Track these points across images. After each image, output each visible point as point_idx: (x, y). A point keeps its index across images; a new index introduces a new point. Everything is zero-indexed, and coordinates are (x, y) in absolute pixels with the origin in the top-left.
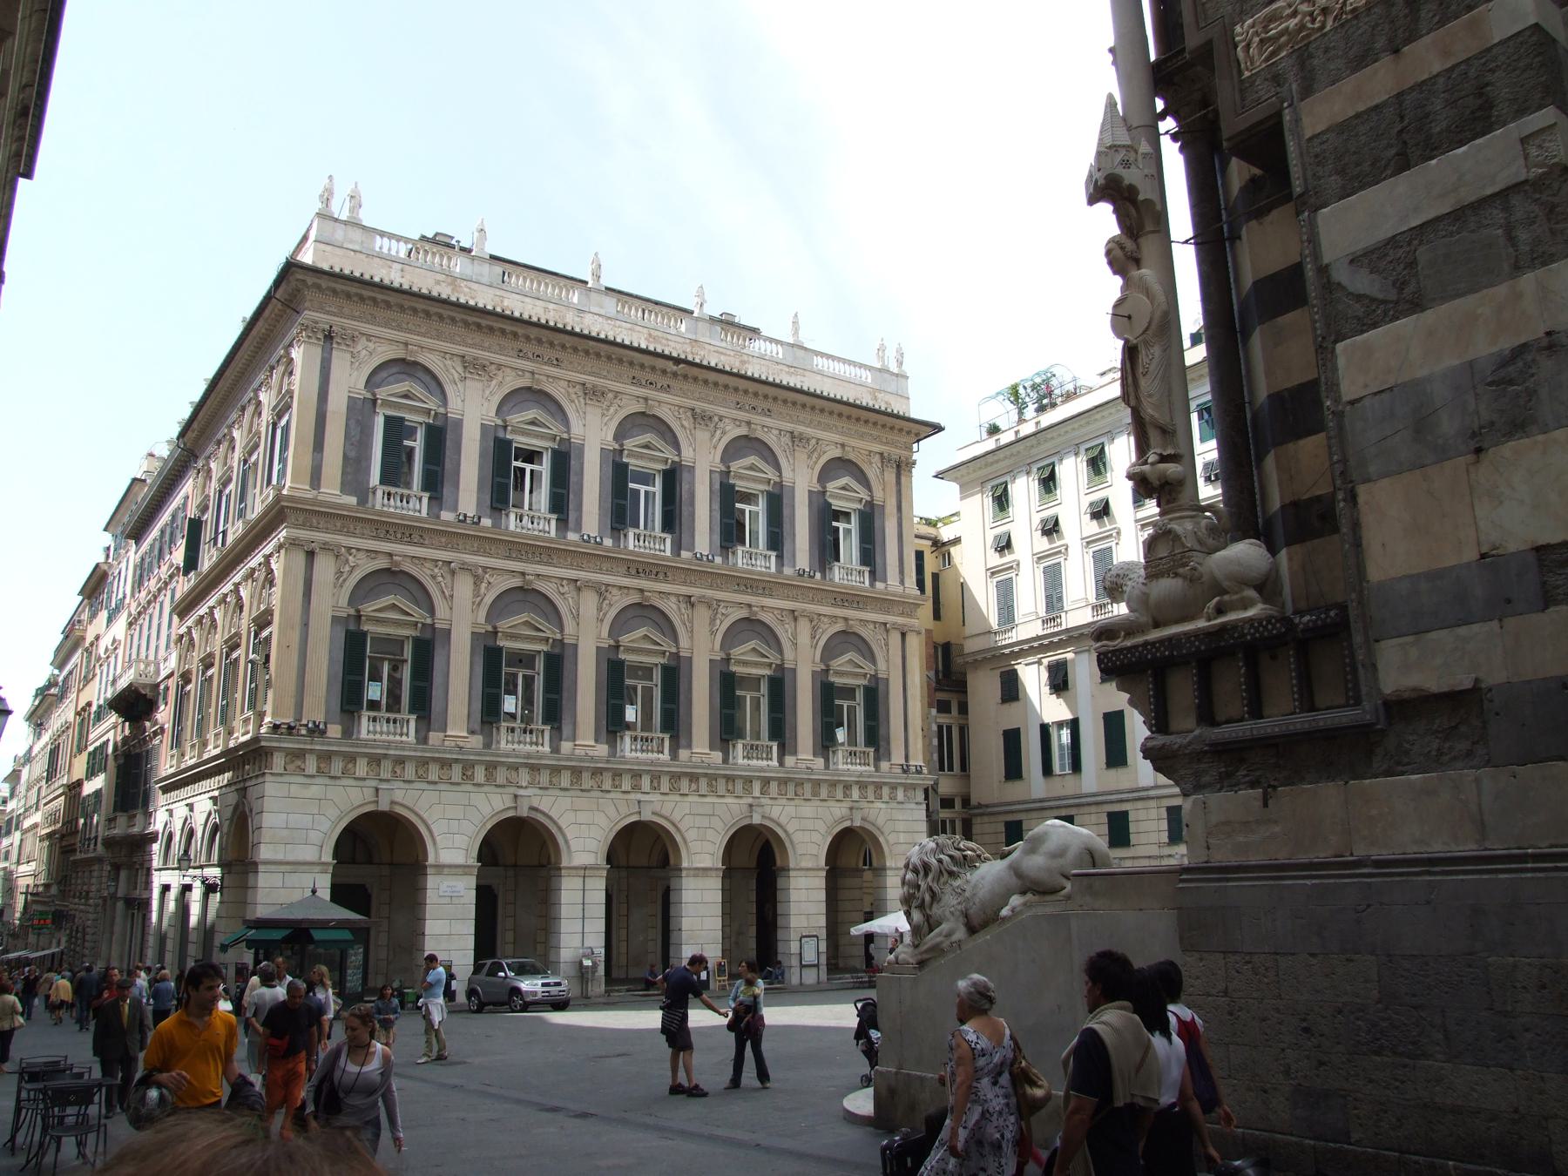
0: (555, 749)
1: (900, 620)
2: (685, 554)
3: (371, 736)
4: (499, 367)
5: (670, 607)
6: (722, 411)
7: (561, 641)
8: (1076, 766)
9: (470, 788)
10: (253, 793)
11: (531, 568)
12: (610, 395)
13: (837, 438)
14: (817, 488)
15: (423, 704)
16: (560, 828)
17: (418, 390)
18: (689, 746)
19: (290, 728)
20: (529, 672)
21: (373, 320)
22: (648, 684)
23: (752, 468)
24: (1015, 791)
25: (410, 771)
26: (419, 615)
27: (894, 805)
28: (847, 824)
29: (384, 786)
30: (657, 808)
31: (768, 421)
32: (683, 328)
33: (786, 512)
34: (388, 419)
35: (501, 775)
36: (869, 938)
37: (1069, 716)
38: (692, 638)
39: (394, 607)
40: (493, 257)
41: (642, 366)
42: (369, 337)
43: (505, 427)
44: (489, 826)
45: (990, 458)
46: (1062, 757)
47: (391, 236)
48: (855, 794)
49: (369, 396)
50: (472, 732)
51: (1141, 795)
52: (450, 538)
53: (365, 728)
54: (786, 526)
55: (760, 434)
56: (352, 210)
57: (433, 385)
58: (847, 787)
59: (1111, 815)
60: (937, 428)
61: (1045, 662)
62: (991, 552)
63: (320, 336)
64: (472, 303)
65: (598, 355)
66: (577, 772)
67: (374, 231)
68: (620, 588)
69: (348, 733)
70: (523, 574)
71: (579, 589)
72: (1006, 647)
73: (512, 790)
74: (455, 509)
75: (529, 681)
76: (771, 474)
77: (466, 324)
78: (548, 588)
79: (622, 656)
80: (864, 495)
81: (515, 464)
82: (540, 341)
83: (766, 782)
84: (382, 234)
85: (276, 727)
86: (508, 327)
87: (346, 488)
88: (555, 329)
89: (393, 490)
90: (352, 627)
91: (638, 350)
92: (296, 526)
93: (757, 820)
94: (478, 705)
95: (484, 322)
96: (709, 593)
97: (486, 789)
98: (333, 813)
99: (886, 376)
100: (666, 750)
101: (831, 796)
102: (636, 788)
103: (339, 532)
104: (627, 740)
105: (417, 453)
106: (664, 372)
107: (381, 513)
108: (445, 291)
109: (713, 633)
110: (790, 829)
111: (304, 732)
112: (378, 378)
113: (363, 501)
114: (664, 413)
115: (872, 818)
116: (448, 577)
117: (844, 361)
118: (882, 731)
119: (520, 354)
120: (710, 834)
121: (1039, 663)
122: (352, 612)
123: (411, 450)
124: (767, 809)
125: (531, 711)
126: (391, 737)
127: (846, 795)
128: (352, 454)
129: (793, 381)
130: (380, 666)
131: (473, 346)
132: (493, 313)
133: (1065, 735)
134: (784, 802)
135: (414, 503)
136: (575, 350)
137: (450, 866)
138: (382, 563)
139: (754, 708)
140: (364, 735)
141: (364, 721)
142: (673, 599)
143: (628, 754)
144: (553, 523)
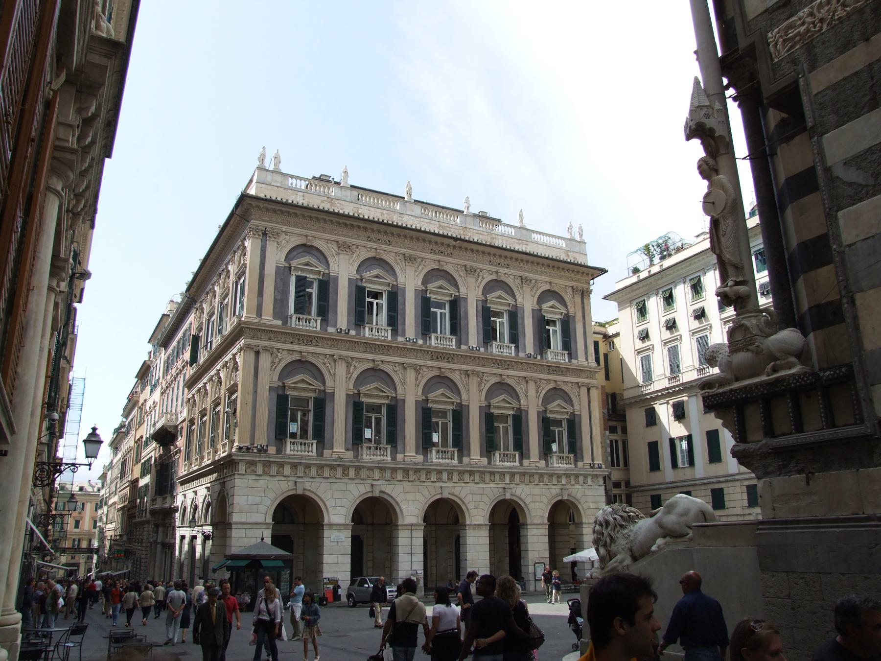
0: (394, 458)
1: (587, 381)
2: (463, 347)
3: (292, 453)
4: (358, 246)
5: (456, 377)
6: (481, 266)
7: (396, 397)
8: (691, 462)
9: (346, 481)
10: (228, 485)
11: (378, 357)
12: (419, 260)
13: (547, 279)
14: (536, 307)
15: (320, 434)
16: (397, 503)
17: (313, 261)
18: (469, 455)
19: (248, 449)
20: (378, 415)
21: (288, 224)
22: (444, 420)
23: (500, 297)
24: (656, 477)
25: (313, 472)
26: (317, 385)
27: (586, 487)
28: (559, 498)
29: (299, 480)
30: (451, 490)
31: (508, 271)
32: (458, 221)
33: (519, 321)
34: (297, 277)
35: (364, 473)
36: (574, 564)
37: (686, 433)
38: (468, 394)
39: (303, 381)
40: (352, 186)
41: (436, 243)
42: (286, 233)
43: (362, 280)
44: (358, 502)
45: (635, 287)
46: (683, 457)
47: (297, 178)
48: (564, 480)
49: (287, 265)
50: (347, 450)
51: (730, 479)
52: (333, 342)
53: (289, 448)
54: (520, 330)
55: (503, 278)
56: (275, 165)
57: (322, 257)
58: (559, 477)
59: (713, 491)
60: (604, 271)
61: (671, 402)
62: (637, 340)
63: (260, 233)
64: (341, 212)
65: (412, 238)
66: (406, 471)
67: (288, 175)
68: (428, 367)
69: (279, 451)
70: (374, 361)
71: (405, 368)
72: (648, 394)
73: (370, 482)
74: (335, 325)
75: (378, 421)
76: (510, 301)
77: (339, 224)
78: (387, 368)
79: (430, 405)
80: (563, 310)
81: (368, 300)
82: (379, 231)
83: (513, 475)
84: (292, 177)
85: (240, 448)
86: (362, 225)
87: (276, 316)
88: (387, 224)
89: (301, 316)
90: (280, 392)
91: (434, 234)
92: (250, 338)
93: (508, 496)
94: (350, 435)
95: (348, 222)
96: (478, 369)
97: (355, 481)
98: (272, 495)
99: (574, 243)
100: (456, 458)
101: (550, 482)
102: (439, 479)
103: (273, 340)
104: (434, 452)
105: (314, 296)
106: (449, 246)
107: (295, 329)
108: (327, 206)
109: (481, 391)
110: (527, 501)
111: (255, 451)
112: (291, 256)
113: (285, 323)
114: (450, 269)
115: (573, 494)
116: (333, 363)
117: (549, 235)
118: (578, 444)
119: (369, 239)
120: (482, 505)
121: (667, 403)
122: (280, 384)
123: (310, 294)
124: (514, 490)
125: (380, 437)
126: (303, 453)
127: (558, 482)
128: (279, 297)
129: (521, 248)
130: (296, 414)
131: (344, 235)
132: (353, 217)
133: (684, 444)
134: (524, 486)
135: (313, 323)
136: (399, 235)
137: (337, 525)
138: (296, 357)
139: (505, 433)
140: (288, 452)
141: (288, 444)
142: (458, 372)
143: (434, 460)
144: (390, 332)
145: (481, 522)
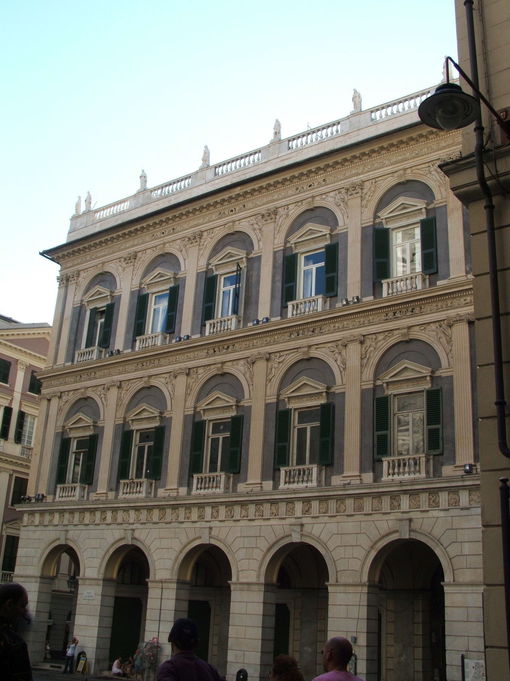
3: (60, 499)
5: (239, 370)
9: (103, 527)
31: (324, 189)
93: (296, 538)
101: (376, 511)
134: (326, 519)
145: (254, 579)
